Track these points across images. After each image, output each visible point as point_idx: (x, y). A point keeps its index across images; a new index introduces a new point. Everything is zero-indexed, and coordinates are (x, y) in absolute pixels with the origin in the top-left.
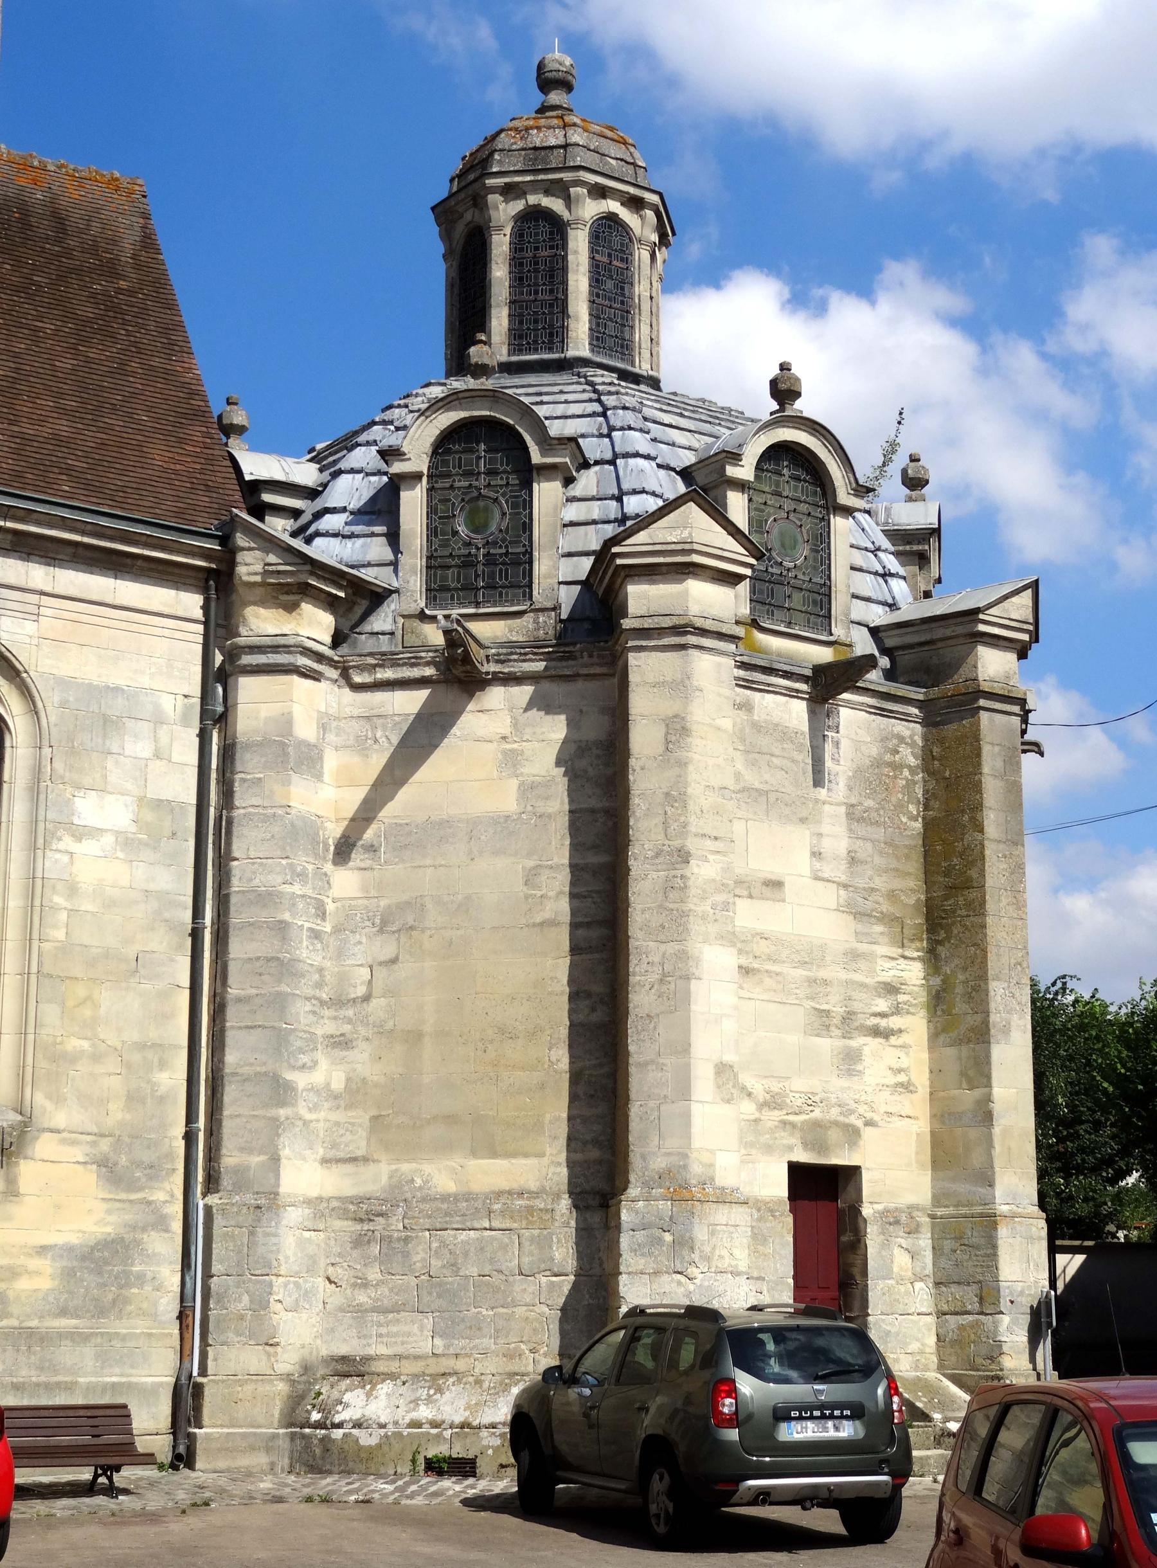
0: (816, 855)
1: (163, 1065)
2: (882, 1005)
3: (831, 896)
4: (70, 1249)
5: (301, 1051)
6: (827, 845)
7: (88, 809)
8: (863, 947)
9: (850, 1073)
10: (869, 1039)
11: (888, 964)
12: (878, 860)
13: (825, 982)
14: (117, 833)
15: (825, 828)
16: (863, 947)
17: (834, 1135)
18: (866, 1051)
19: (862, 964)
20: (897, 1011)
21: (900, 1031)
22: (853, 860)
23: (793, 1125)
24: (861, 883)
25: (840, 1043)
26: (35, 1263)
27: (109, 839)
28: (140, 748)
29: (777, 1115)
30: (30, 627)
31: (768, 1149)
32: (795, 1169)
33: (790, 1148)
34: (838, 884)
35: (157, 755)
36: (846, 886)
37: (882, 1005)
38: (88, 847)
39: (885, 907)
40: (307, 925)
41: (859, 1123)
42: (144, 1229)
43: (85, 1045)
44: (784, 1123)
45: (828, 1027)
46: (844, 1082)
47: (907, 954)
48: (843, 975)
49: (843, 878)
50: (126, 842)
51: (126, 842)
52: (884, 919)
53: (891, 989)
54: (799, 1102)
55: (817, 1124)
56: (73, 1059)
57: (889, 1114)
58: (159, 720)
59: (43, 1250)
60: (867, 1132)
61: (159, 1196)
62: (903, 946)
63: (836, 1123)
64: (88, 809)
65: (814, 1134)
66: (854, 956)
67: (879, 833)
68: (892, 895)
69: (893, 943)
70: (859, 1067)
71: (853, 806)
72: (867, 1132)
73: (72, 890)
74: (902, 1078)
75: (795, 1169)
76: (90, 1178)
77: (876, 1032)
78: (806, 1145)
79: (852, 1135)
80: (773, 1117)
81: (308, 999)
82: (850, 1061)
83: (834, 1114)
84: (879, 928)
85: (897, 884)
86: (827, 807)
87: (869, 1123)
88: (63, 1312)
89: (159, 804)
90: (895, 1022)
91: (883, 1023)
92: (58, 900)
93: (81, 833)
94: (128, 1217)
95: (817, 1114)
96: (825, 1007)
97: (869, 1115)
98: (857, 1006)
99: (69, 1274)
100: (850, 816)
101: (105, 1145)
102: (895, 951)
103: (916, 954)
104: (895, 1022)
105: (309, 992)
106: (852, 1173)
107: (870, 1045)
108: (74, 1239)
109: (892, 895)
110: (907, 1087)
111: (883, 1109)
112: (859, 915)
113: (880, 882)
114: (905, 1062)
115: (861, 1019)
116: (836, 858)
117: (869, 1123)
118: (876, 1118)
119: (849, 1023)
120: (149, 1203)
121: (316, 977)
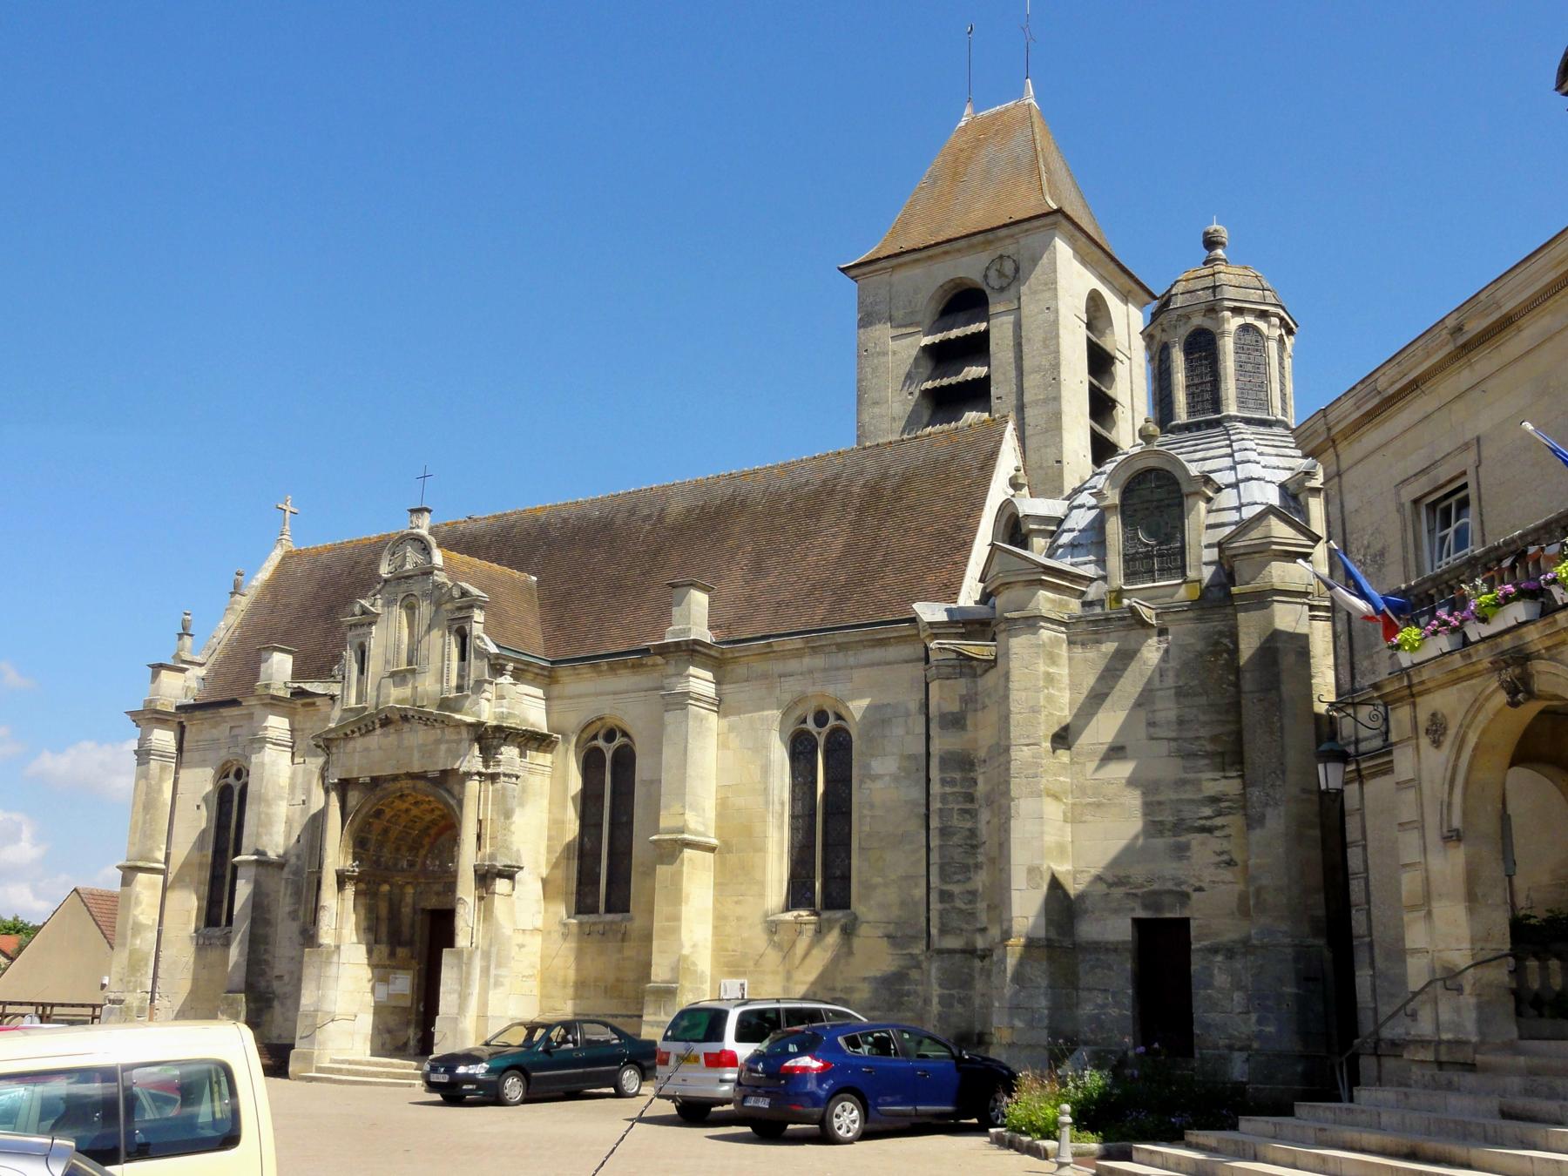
0: (1151, 724)
2: (1207, 811)
3: (1163, 748)
4: (875, 978)
6: (1161, 716)
7: (878, 766)
8: (1191, 776)
9: (1180, 858)
11: (1212, 784)
12: (1202, 718)
13: (1160, 803)
15: (1159, 706)
16: (1191, 776)
17: (1167, 900)
18: (1194, 843)
19: (1188, 787)
20: (1219, 814)
22: (1181, 722)
23: (1135, 895)
25: (1172, 840)
28: (900, 731)
29: (1122, 890)
30: (849, 686)
31: (1116, 911)
32: (1137, 922)
33: (1133, 909)
36: (1174, 740)
37: (1207, 811)
38: (878, 785)
39: (1209, 747)
40: (957, 807)
41: (1190, 890)
43: (880, 880)
46: (1174, 865)
48: (1174, 796)
49: (1173, 735)
50: (896, 779)
51: (896, 779)
52: (1208, 755)
53: (1214, 800)
55: (1154, 893)
58: (908, 714)
59: (865, 979)
60: (1195, 896)
61: (916, 951)
63: (1170, 892)
64: (878, 766)
65: (1152, 899)
66: (1181, 783)
67: (1203, 700)
68: (1214, 739)
72: (1195, 896)
73: (872, 806)
74: (1225, 857)
75: (1137, 922)
76: (884, 943)
77: (1203, 829)
78: (1145, 907)
79: (1184, 897)
80: (1118, 892)
82: (1181, 851)
83: (1170, 885)
85: (1218, 730)
87: (1200, 889)
89: (909, 757)
90: (1219, 821)
91: (1208, 823)
92: (866, 812)
93: (875, 778)
94: (902, 963)
95: (1156, 887)
98: (1186, 815)
101: (891, 928)
102: (1218, 775)
104: (1219, 821)
106: (1185, 923)
107: (1196, 839)
108: (878, 974)
109: (1214, 739)
110: (1230, 863)
113: (1203, 732)
114: (1226, 846)
115: (1189, 822)
116: (1169, 723)
117: (1200, 889)
119: (1179, 827)
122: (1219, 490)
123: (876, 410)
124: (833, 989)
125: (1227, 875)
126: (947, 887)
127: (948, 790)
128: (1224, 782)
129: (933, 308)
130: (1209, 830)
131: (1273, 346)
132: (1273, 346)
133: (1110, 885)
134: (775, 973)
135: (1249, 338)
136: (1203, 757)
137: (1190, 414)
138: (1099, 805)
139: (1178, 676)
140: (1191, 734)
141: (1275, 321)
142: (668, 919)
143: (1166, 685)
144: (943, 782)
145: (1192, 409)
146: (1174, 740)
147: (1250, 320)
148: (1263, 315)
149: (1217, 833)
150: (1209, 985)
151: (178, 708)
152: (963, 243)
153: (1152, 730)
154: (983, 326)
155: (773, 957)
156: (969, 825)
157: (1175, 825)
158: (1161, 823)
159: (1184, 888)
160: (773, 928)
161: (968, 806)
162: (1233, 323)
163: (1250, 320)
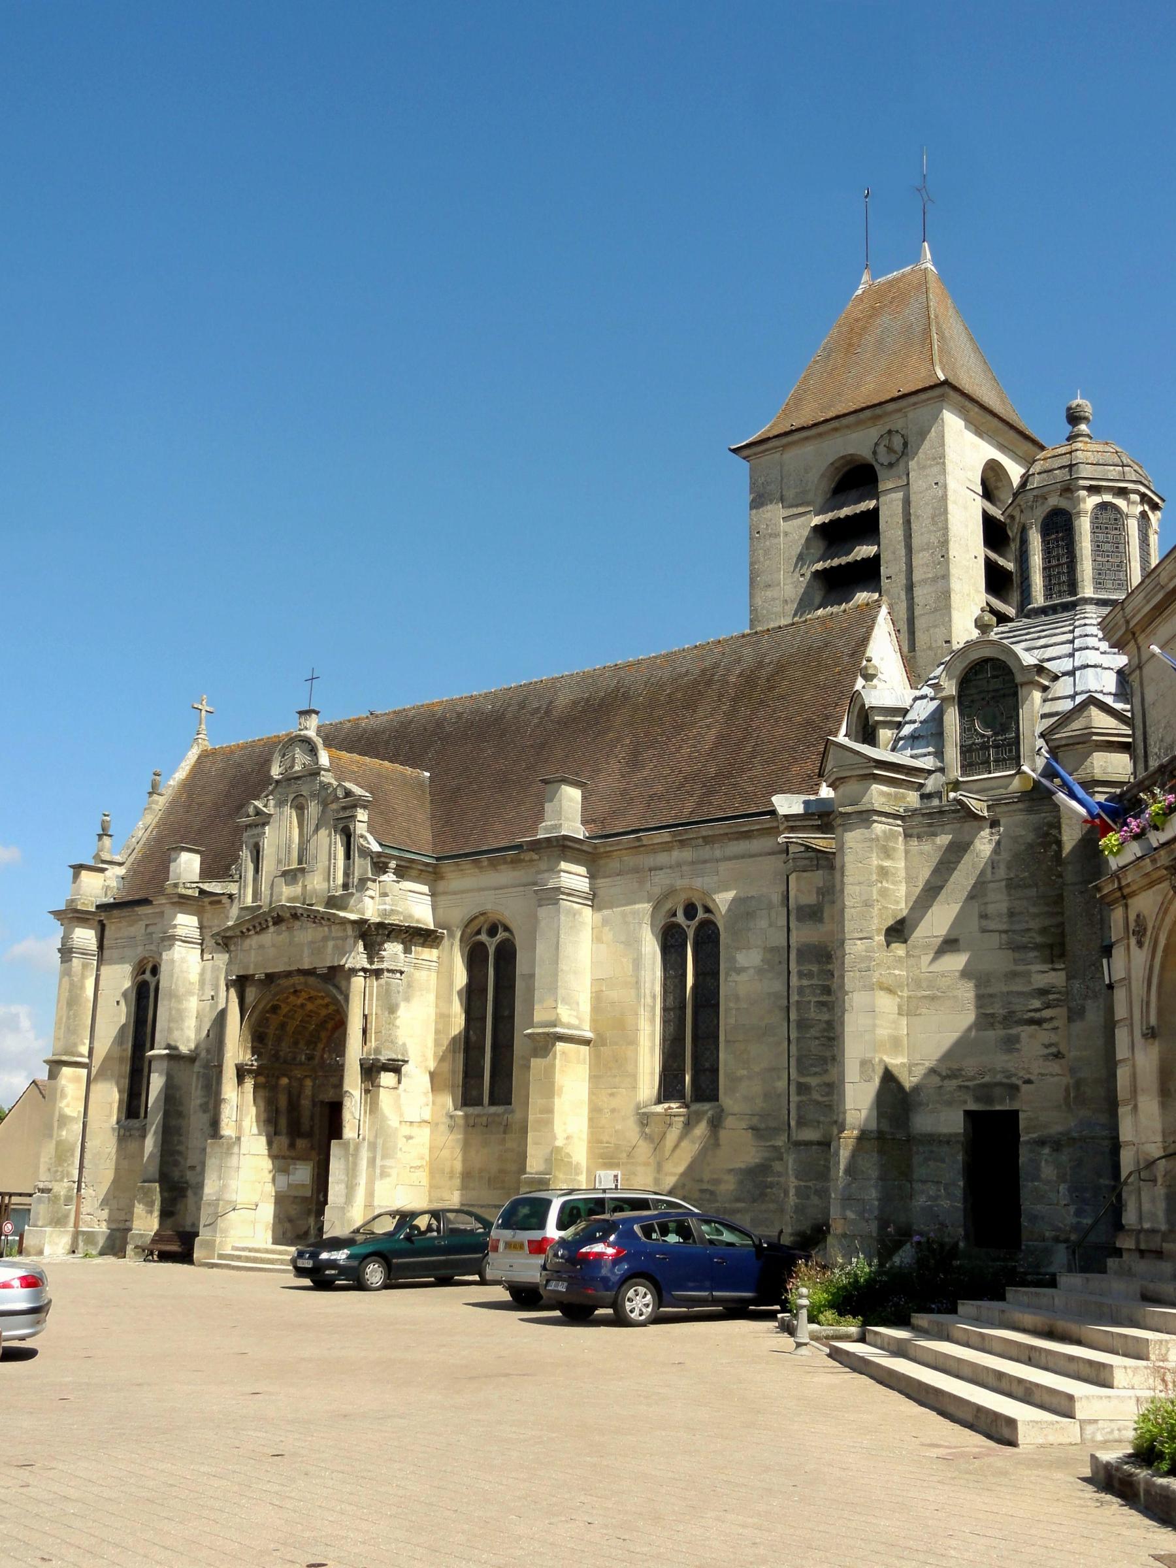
0: (984, 916)
1: (779, 1078)
2: (1036, 1004)
5: (812, 1065)
6: (991, 909)
7: (742, 959)
8: (1021, 968)
9: (1010, 1051)
10: (1025, 1027)
11: (1040, 977)
12: (1033, 910)
13: (991, 996)
14: (755, 968)
16: (1021, 968)
17: (998, 1091)
18: (1023, 1034)
21: (1052, 1018)
22: (1011, 914)
23: (967, 1087)
24: (1017, 927)
25: (1001, 1033)
26: (726, 1177)
27: (752, 971)
28: (763, 923)
31: (949, 1103)
32: (968, 1113)
33: (965, 1102)
34: (1001, 932)
35: (770, 925)
37: (1036, 1004)
38: (744, 977)
39: (1039, 939)
41: (1019, 1082)
42: (773, 1160)
43: (745, 1072)
44: (960, 1087)
45: (992, 1025)
46: (1006, 1057)
47: (1057, 966)
48: (1005, 989)
49: (1005, 927)
52: (1038, 947)
53: (1042, 992)
54: (972, 1074)
55: (984, 1085)
56: (740, 1079)
57: (1042, 1075)
58: (770, 906)
59: (730, 1171)
60: (1025, 1088)
61: (780, 1143)
62: (1052, 962)
63: (1000, 1084)
64: (742, 959)
65: (984, 1092)
66: (1013, 975)
67: (1032, 892)
69: (1044, 962)
70: (1017, 1046)
71: (1011, 879)
72: (1025, 1088)
73: (737, 998)
74: (1053, 1050)
75: (968, 1113)
78: (977, 1099)
79: (1013, 1089)
81: (816, 1038)
82: (1010, 1044)
83: (999, 1078)
84: (1032, 954)
85: (1047, 922)
86: (991, 885)
87: (1029, 1082)
88: (738, 1200)
90: (1047, 1013)
91: (1037, 1015)
92: (732, 1005)
93: (739, 971)
94: (767, 1155)
95: (987, 1079)
96: (991, 1011)
97: (1027, 1077)
98: (1017, 1008)
99: (741, 1182)
100: (1008, 886)
102: (1045, 967)
103: (1063, 966)
104: (1047, 1013)
105: (818, 1035)
106: (1014, 1114)
107: (1025, 1032)
108: (743, 1166)
109: (1043, 931)
110: (1058, 1056)
111: (1036, 1071)
112: (1016, 948)
113: (1032, 925)
114: (1054, 1038)
116: (1000, 915)
117: (1029, 1082)
118: (1033, 1078)
119: (1010, 1019)
120: (773, 1146)
121: (824, 1025)
122: (1056, 678)
123: (769, 594)
124: (701, 1181)
125: (1055, 1067)
126: (802, 1080)
127: (805, 982)
128: (1053, 973)
129: (827, 486)
130: (1038, 1022)
131: (1133, 526)
132: (1133, 526)
133: (944, 1078)
134: (647, 1164)
135: (1106, 516)
136: (1032, 949)
137: (1048, 595)
138: (933, 998)
139: (1009, 868)
140: (1024, 926)
141: (1136, 498)
142: (541, 1112)
143: (997, 877)
144: (801, 975)
145: (1049, 591)
146: (1006, 932)
147: (1108, 498)
148: (1122, 492)
149: (1045, 1026)
150: (1036, 1177)
151: (98, 907)
152: (851, 419)
153: (984, 923)
154: (872, 504)
155: (644, 1150)
156: (826, 1017)
157: (1005, 1018)
158: (992, 1015)
159: (1014, 1080)
160: (644, 1119)
161: (824, 998)
162: (1090, 502)
163: (1108, 498)
